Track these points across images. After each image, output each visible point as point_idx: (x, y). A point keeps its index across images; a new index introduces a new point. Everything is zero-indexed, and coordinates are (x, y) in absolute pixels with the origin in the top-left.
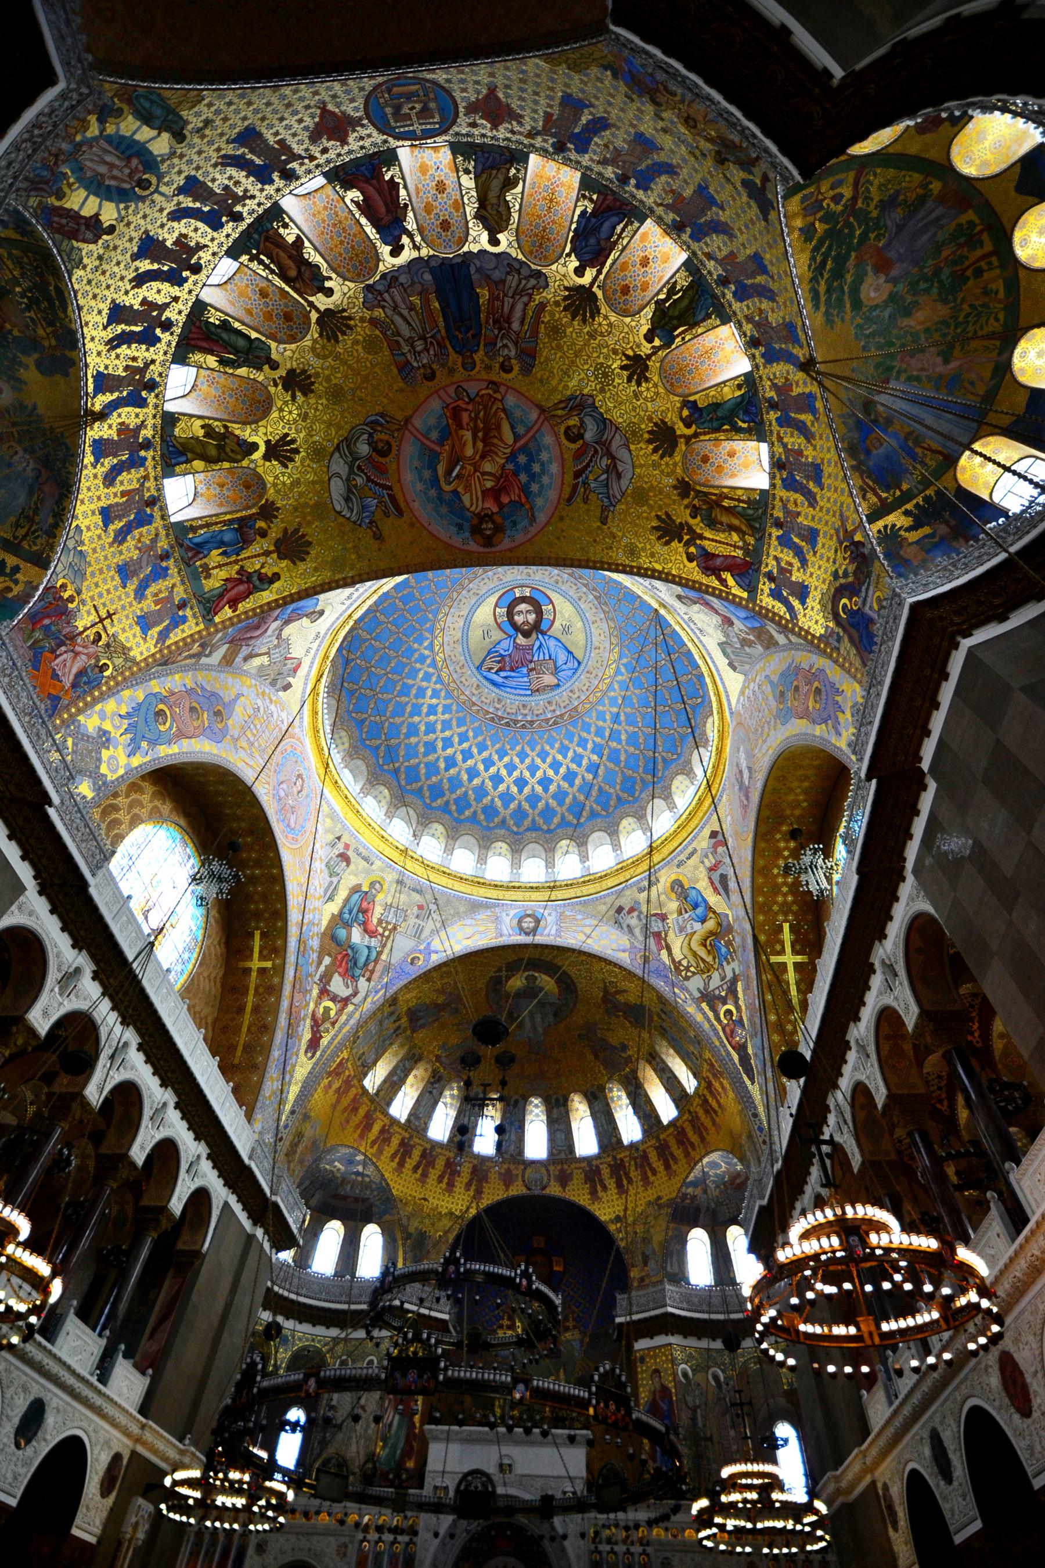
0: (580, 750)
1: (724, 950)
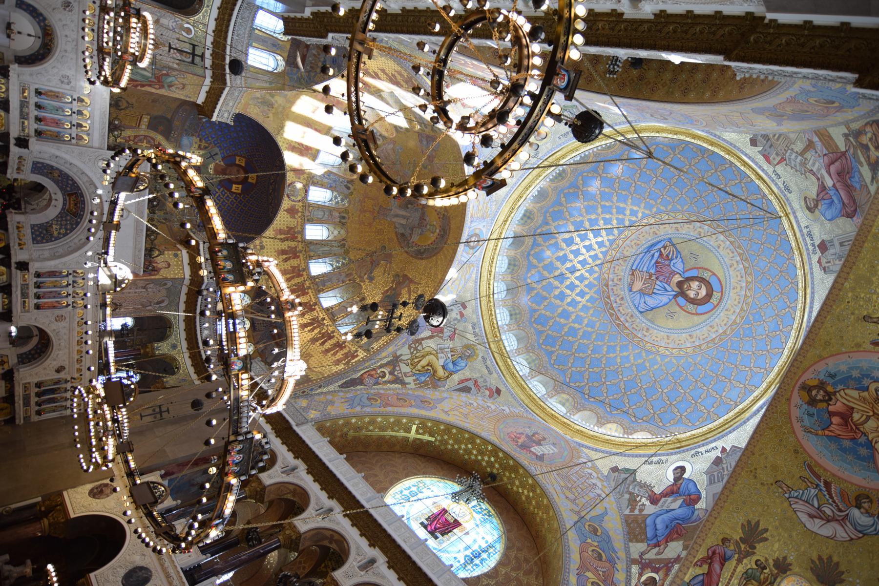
0: (578, 290)
1: (423, 379)
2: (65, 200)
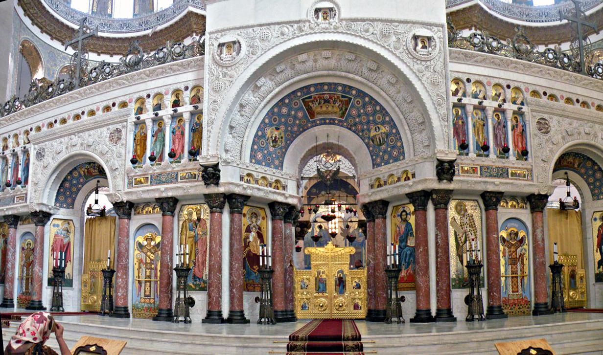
2: (323, 122)
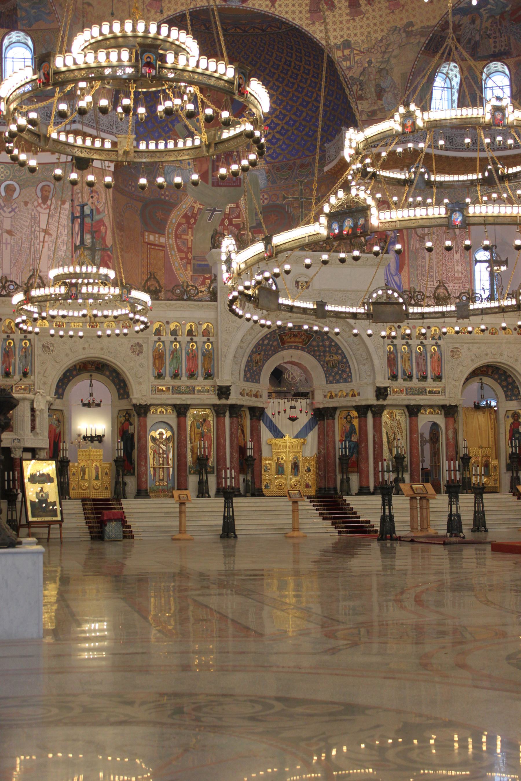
2: (290, 348)
